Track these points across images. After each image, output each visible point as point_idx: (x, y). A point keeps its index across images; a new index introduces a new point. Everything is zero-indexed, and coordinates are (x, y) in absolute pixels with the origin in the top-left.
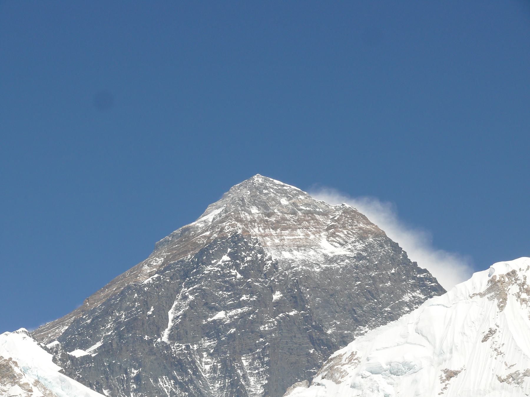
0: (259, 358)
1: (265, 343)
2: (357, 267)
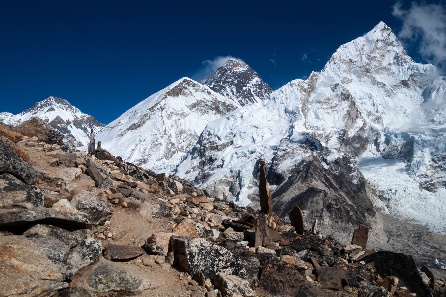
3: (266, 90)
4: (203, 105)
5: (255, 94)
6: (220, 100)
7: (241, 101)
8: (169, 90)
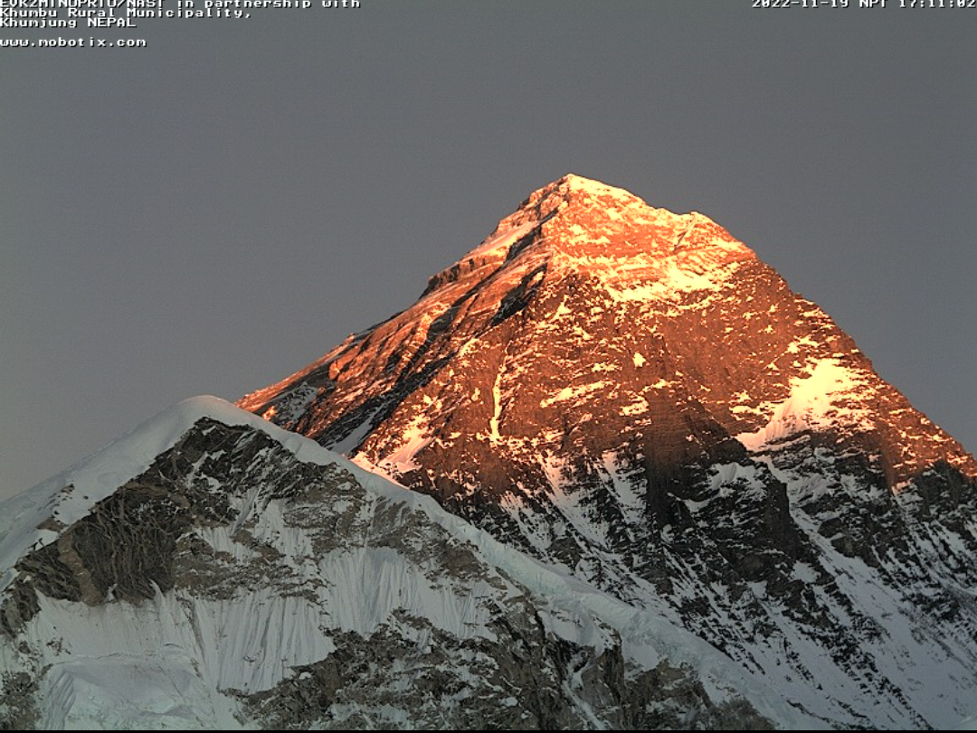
0: (627, 455)
1: (633, 433)
2: (728, 306)
4: (401, 686)
5: (827, 529)
6: (568, 633)
7: (701, 606)
8: (49, 537)
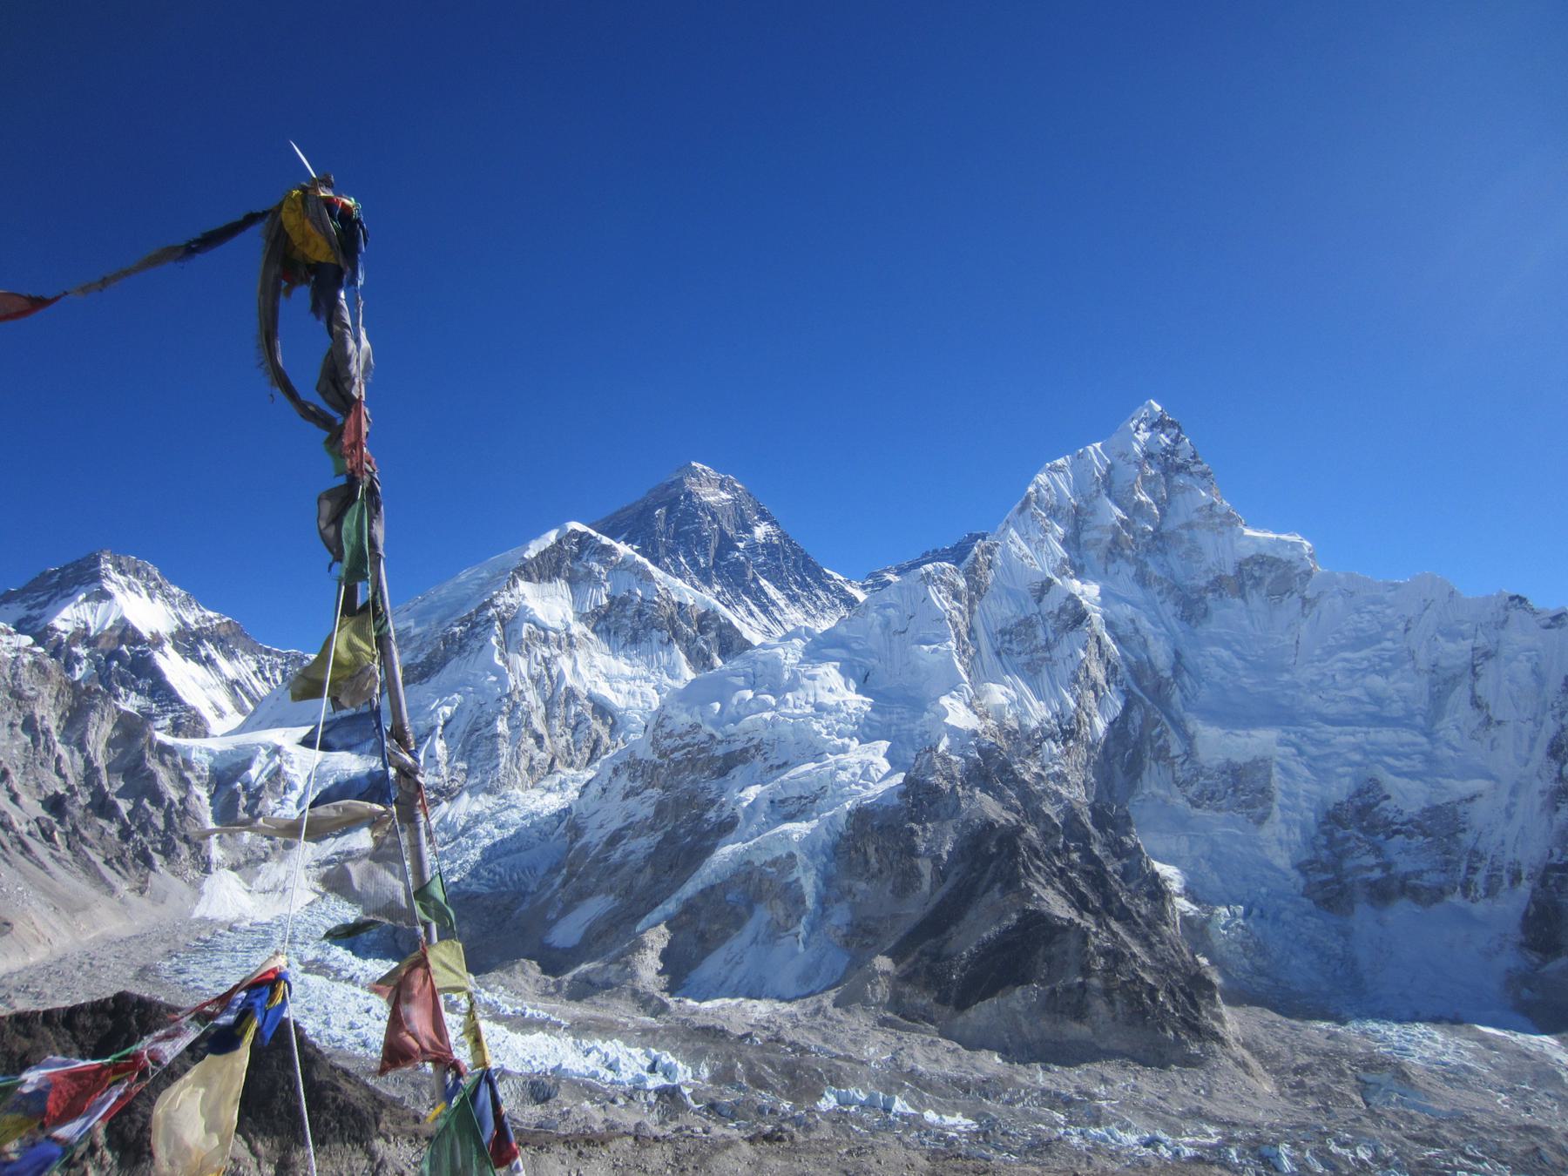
3: (795, 565)
